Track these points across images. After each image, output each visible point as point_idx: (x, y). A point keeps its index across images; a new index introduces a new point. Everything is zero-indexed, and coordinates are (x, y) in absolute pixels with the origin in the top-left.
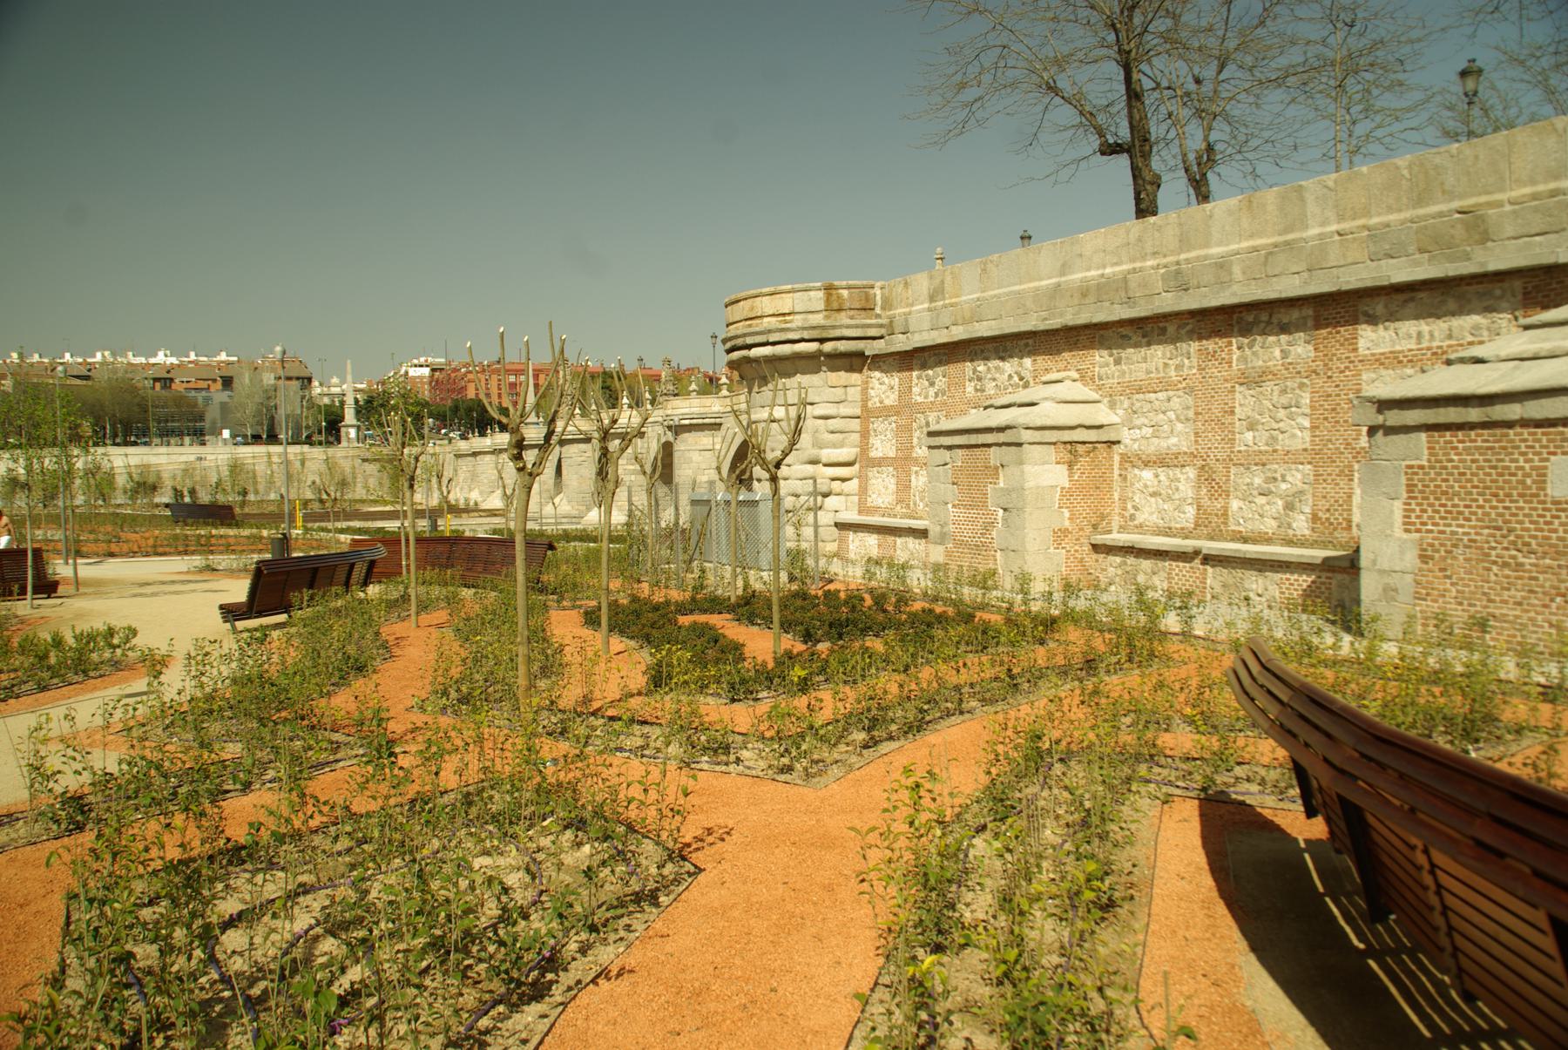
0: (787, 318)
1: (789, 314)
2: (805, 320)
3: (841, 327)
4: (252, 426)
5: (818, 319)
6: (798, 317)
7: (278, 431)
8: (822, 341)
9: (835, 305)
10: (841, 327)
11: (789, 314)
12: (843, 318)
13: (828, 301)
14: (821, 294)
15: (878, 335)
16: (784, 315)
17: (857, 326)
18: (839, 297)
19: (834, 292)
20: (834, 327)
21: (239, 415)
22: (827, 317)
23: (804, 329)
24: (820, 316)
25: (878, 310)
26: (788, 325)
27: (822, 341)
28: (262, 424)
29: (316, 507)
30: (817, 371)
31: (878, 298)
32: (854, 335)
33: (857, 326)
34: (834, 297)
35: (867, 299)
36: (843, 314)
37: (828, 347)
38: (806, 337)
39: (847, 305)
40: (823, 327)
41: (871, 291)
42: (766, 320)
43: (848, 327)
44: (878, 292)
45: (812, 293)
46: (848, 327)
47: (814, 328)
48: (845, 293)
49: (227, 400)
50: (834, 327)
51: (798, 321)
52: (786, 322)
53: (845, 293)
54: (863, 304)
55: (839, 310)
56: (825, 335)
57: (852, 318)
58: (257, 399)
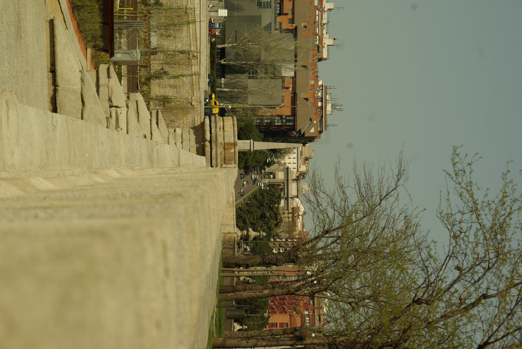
0: (222, 130)
1: (224, 130)
2: (220, 135)
3: (217, 148)
4: (233, 47)
5: (220, 140)
6: (222, 133)
7: (228, 76)
8: (210, 142)
9: (226, 147)
10: (217, 148)
11: (224, 130)
12: (220, 150)
13: (229, 144)
14: (232, 141)
15: (213, 165)
16: (223, 128)
17: (216, 154)
18: (230, 148)
19: (233, 146)
20: (216, 145)
21: (246, 35)
22: (221, 143)
23: (216, 134)
24: (222, 141)
25: (224, 165)
26: (218, 128)
27: (210, 142)
28: (237, 59)
29: (142, 73)
30: (197, 143)
31: (230, 166)
32: (212, 154)
33: (216, 154)
34: (230, 146)
35: (229, 160)
36: (223, 150)
37: (207, 144)
38: (212, 135)
39: (227, 152)
40: (216, 141)
41: (233, 162)
42: (222, 123)
43: (216, 151)
44: (233, 165)
45: (233, 138)
46: (216, 151)
47: (216, 137)
48: (232, 151)
49: (265, 23)
50: (216, 145)
51: (220, 133)
52: (220, 129)
53: (232, 151)
54: (227, 158)
55: (224, 149)
56: (213, 142)
57: (221, 154)
58: (264, 56)
